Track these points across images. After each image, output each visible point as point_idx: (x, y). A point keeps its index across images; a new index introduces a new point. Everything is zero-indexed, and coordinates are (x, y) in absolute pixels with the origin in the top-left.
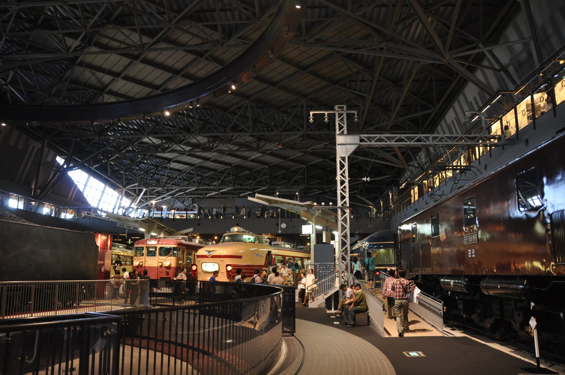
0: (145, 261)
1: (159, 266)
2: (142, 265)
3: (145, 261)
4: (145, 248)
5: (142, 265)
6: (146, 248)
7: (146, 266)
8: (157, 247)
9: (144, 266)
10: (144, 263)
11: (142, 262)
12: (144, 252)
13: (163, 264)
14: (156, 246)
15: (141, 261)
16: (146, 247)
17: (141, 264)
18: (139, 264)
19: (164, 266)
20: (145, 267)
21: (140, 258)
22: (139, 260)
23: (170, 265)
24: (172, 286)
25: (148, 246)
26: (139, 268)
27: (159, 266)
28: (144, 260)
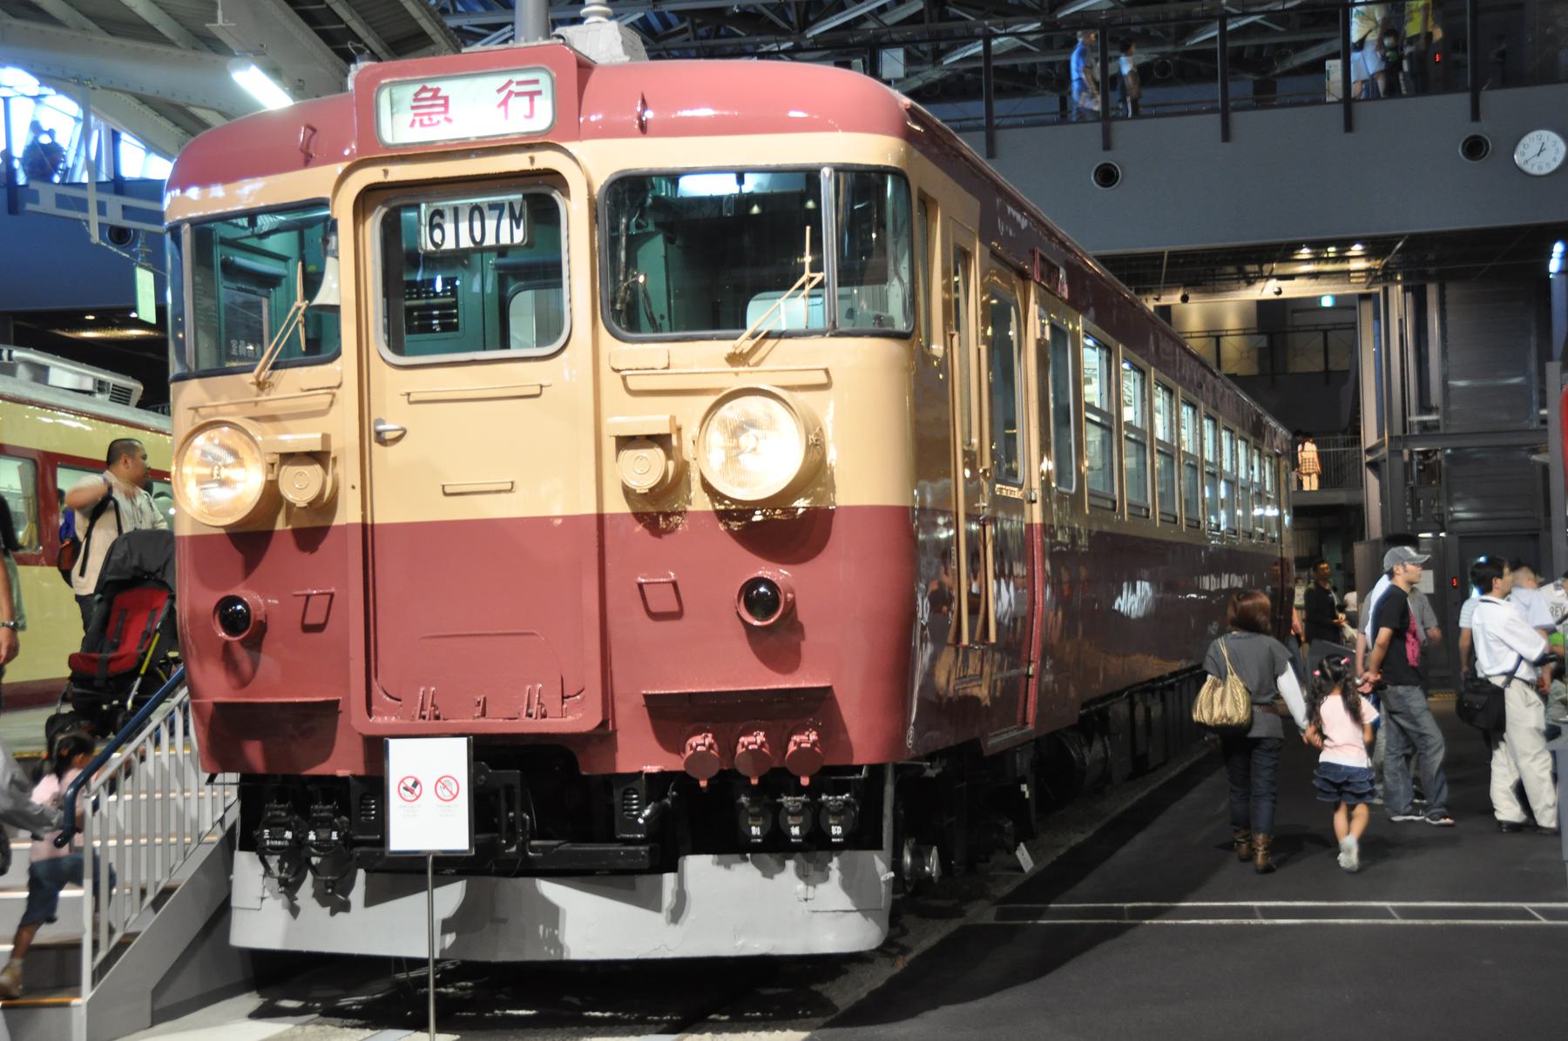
0: (373, 437)
1: (616, 505)
2: (324, 506)
3: (373, 437)
4: (343, 211)
5: (324, 506)
6: (373, 227)
7: (384, 515)
8: (554, 178)
9: (348, 513)
10: (347, 472)
11: (319, 457)
12: (336, 288)
13: (683, 469)
14: (545, 160)
15: (303, 438)
16: (367, 199)
17: (300, 486)
18: (272, 497)
19: (700, 502)
20: (367, 531)
21: (274, 400)
22: (260, 432)
23: (815, 474)
24: (863, 837)
25: (399, 173)
26: (281, 554)
27: (616, 505)
28: (342, 430)
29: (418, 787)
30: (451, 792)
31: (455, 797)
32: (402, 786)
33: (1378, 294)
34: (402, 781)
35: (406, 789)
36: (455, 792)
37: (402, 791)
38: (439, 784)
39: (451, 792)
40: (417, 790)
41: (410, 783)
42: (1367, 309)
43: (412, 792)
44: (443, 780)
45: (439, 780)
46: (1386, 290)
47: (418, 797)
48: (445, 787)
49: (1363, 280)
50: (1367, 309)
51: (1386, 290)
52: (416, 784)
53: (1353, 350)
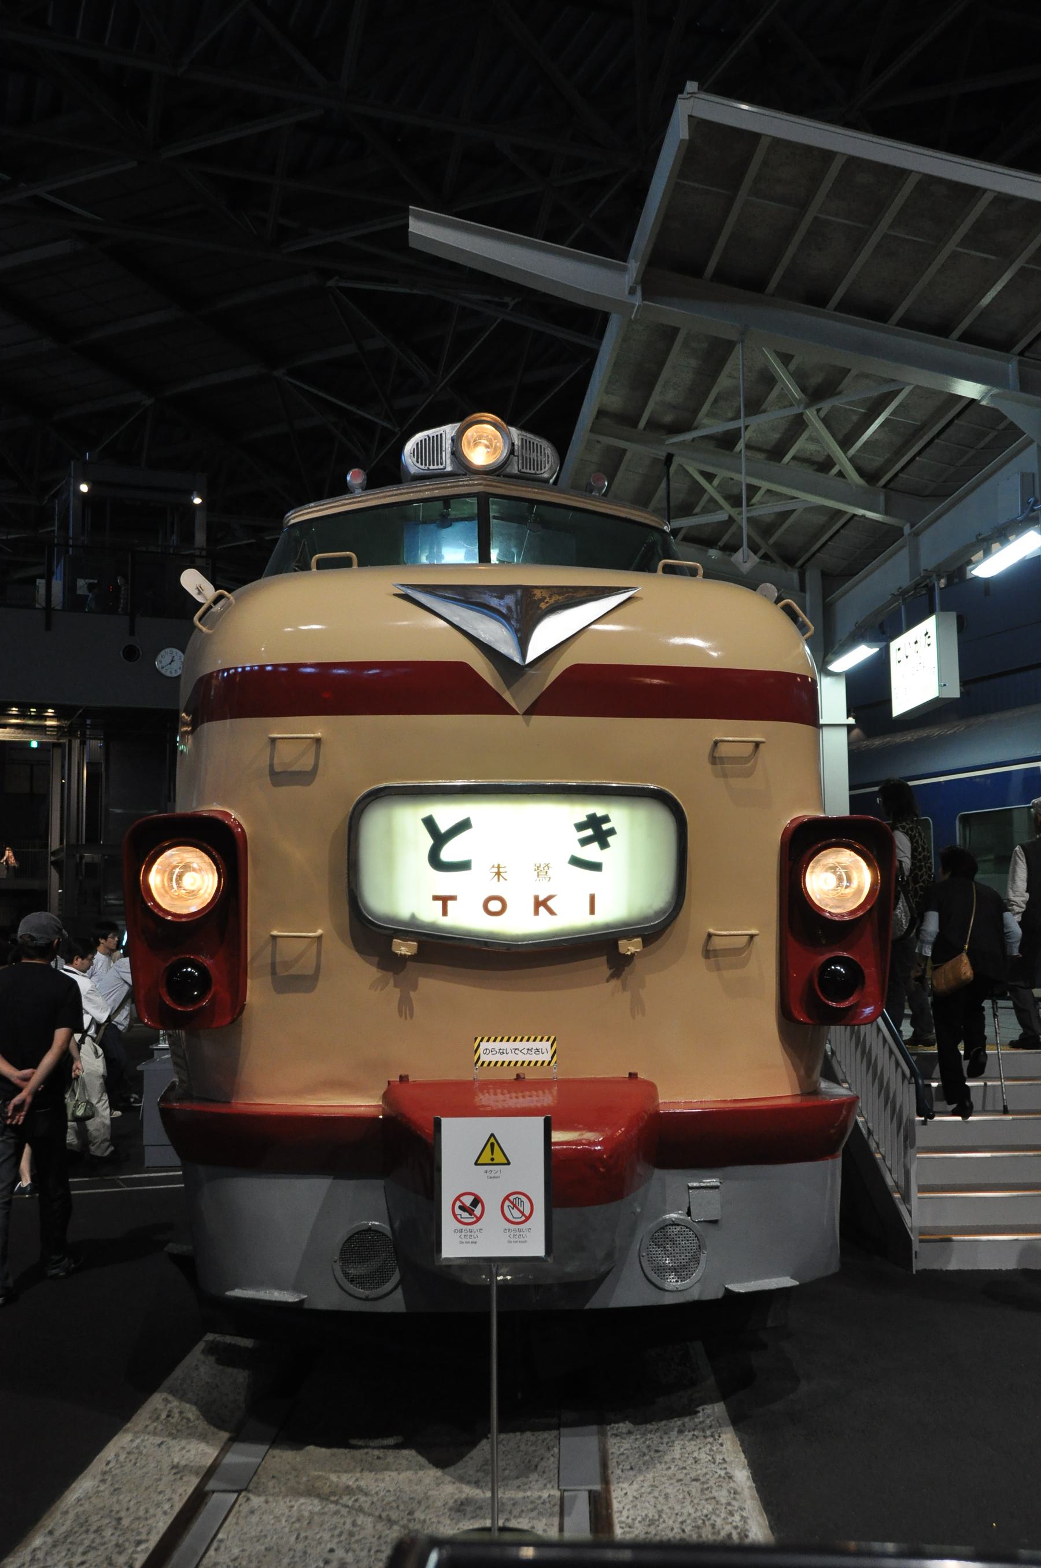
29: (480, 1206)
30: (522, 1213)
31: (527, 1218)
32: (458, 1204)
33: (64, 744)
34: (458, 1198)
35: (463, 1208)
36: (527, 1213)
37: (458, 1211)
38: (507, 1203)
39: (522, 1213)
40: (478, 1211)
41: (468, 1200)
42: (57, 753)
43: (471, 1212)
44: (511, 1198)
45: (507, 1198)
46: (70, 742)
47: (478, 1219)
48: (515, 1206)
49: (55, 733)
50: (57, 753)
51: (70, 742)
52: (477, 1201)
53: (48, 781)
